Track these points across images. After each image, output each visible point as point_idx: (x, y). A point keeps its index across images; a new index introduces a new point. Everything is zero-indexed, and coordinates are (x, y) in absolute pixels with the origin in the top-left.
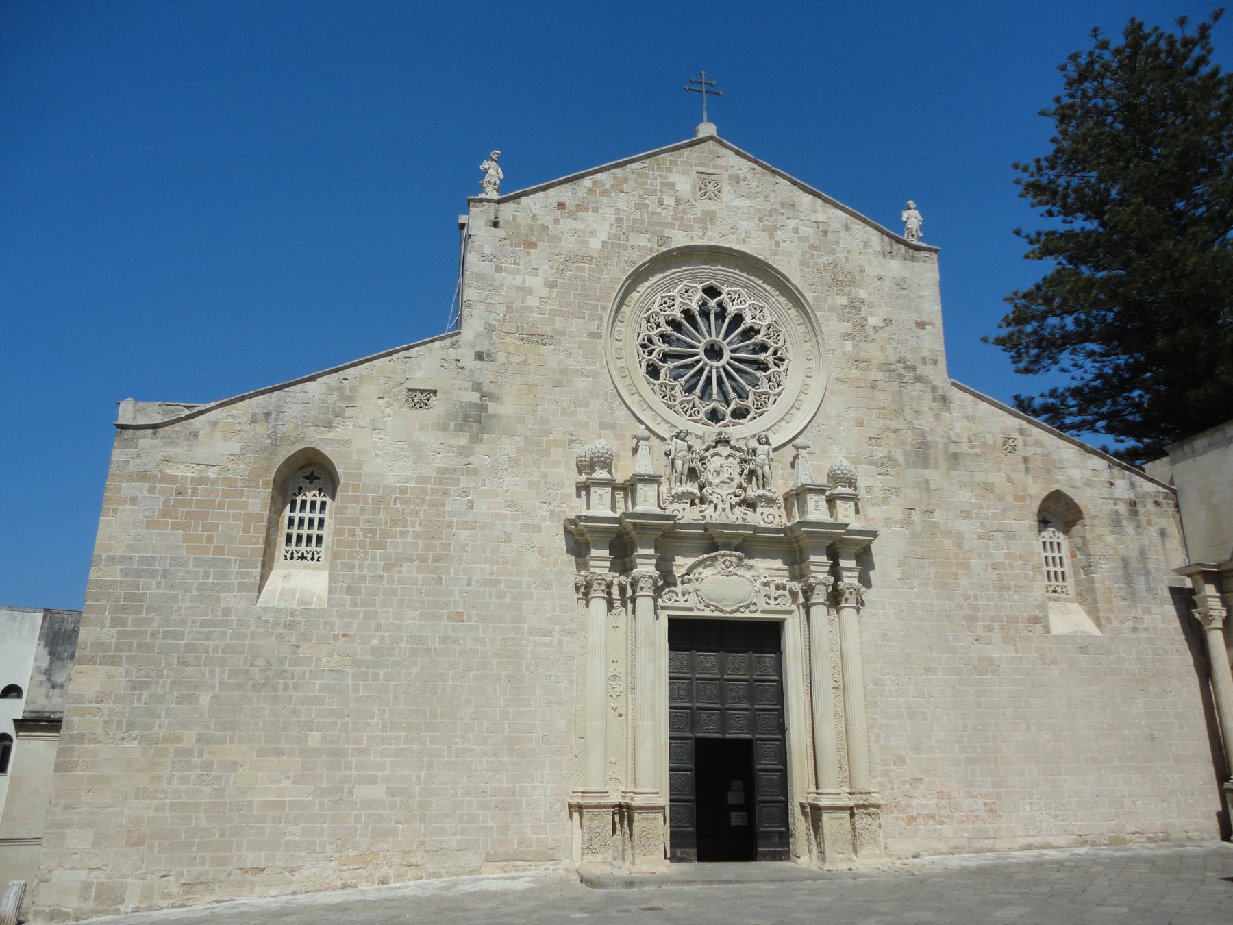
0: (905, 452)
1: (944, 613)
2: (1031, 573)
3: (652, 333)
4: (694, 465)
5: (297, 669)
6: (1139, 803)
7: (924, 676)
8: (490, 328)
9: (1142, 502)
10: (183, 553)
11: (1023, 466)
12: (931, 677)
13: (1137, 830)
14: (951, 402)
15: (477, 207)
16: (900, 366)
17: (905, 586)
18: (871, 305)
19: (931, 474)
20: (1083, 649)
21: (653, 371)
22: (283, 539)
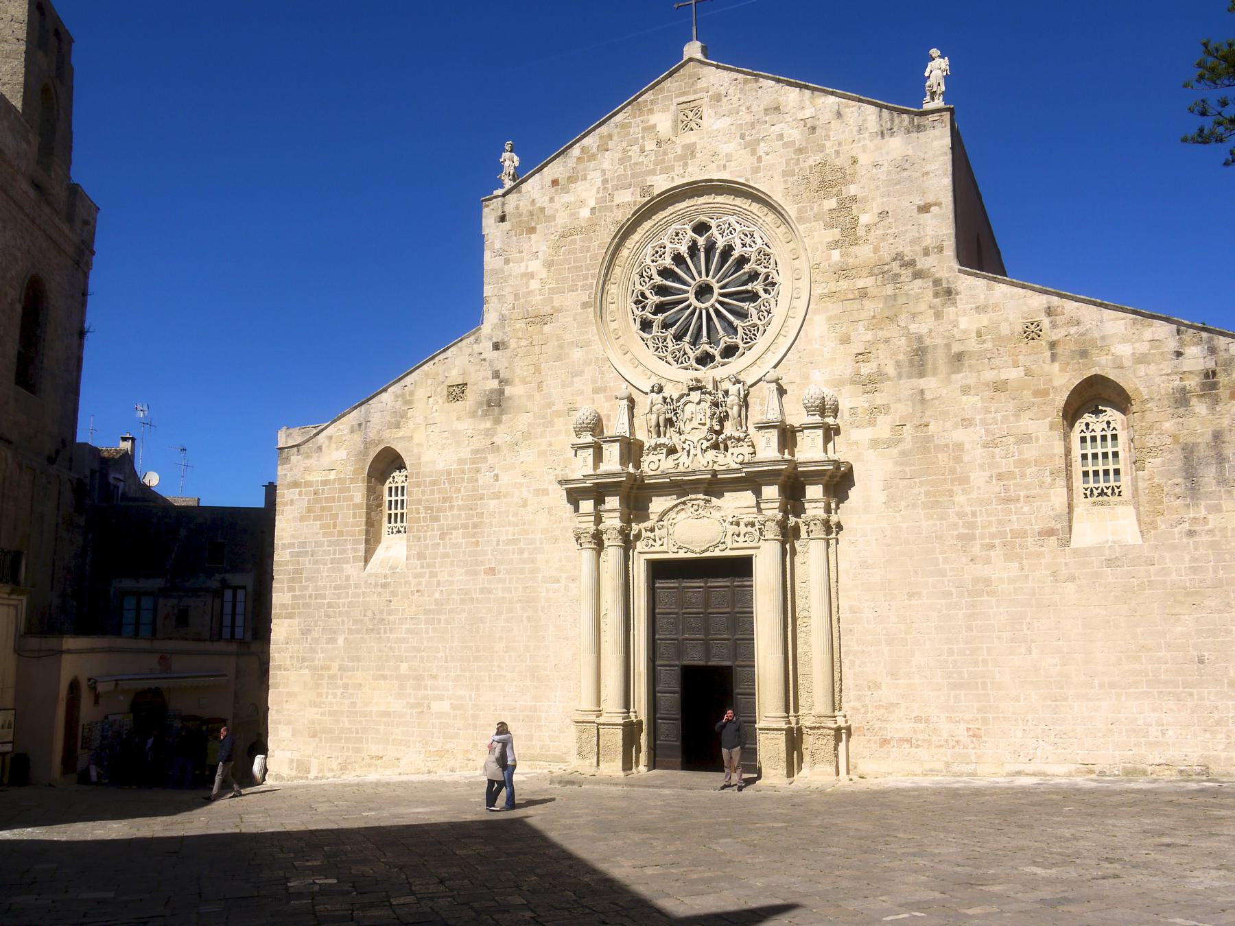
0: (898, 364)
1: (934, 534)
2: (1049, 480)
3: (643, 288)
4: (668, 416)
5: (391, 618)
6: (1170, 733)
7: (906, 602)
8: (503, 318)
9: (1225, 370)
10: (320, 538)
11: (1048, 354)
12: (913, 602)
13: (1164, 762)
14: (957, 294)
15: (488, 206)
16: (895, 265)
17: (891, 510)
18: (865, 200)
19: (930, 384)
20: (1112, 562)
21: (646, 325)
22: (385, 519)
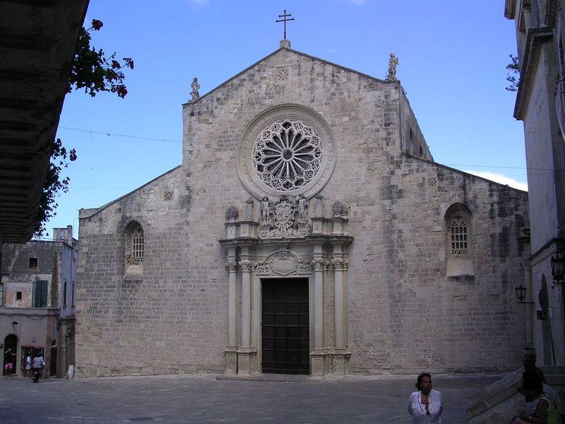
21: (260, 168)
